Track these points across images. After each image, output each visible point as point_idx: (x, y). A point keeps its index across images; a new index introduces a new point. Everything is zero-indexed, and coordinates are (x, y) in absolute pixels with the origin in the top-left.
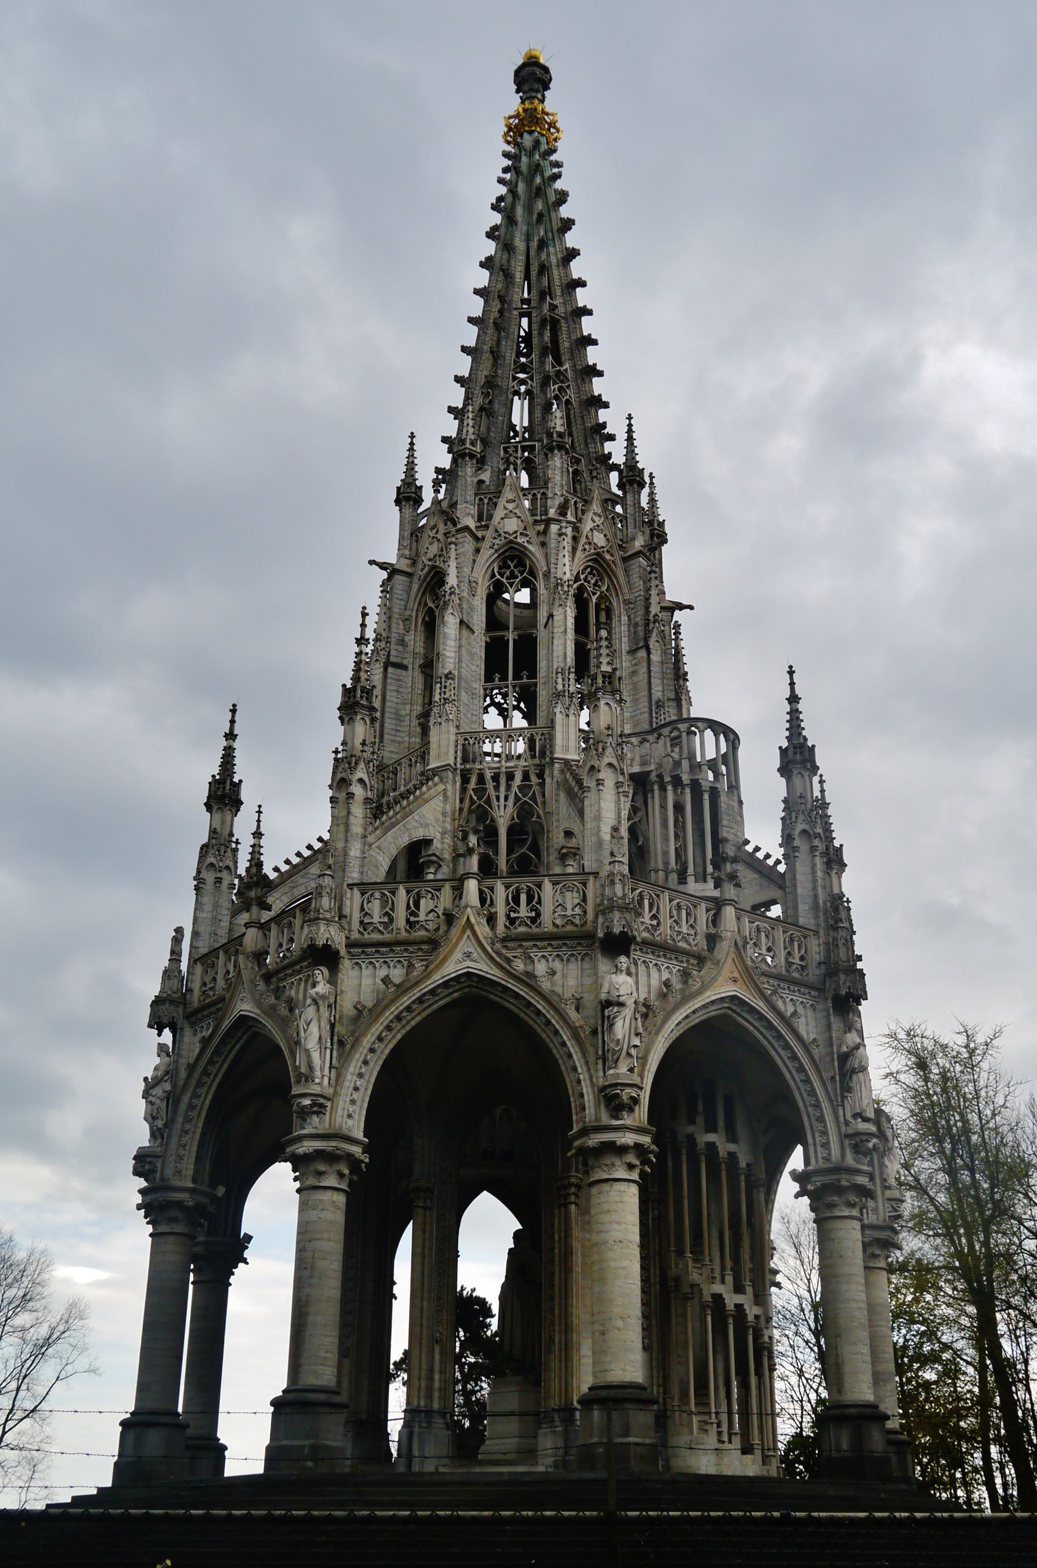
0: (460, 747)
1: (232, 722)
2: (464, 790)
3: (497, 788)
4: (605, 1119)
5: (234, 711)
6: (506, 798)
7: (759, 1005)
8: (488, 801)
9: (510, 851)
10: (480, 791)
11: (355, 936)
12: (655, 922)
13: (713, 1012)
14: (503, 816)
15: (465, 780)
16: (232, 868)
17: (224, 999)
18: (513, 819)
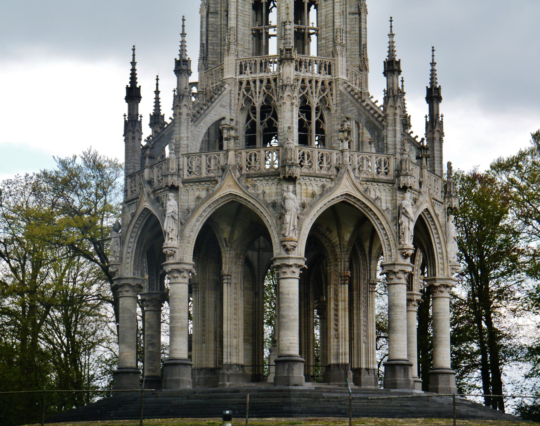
0: (238, 67)
1: (134, 55)
2: (240, 90)
3: (255, 87)
4: (284, 254)
5: (134, 50)
6: (260, 92)
7: (359, 196)
8: (252, 95)
9: (262, 117)
10: (248, 90)
11: (186, 177)
12: (310, 164)
14: (258, 101)
15: (241, 83)
16: (139, 130)
17: (138, 198)
18: (263, 103)
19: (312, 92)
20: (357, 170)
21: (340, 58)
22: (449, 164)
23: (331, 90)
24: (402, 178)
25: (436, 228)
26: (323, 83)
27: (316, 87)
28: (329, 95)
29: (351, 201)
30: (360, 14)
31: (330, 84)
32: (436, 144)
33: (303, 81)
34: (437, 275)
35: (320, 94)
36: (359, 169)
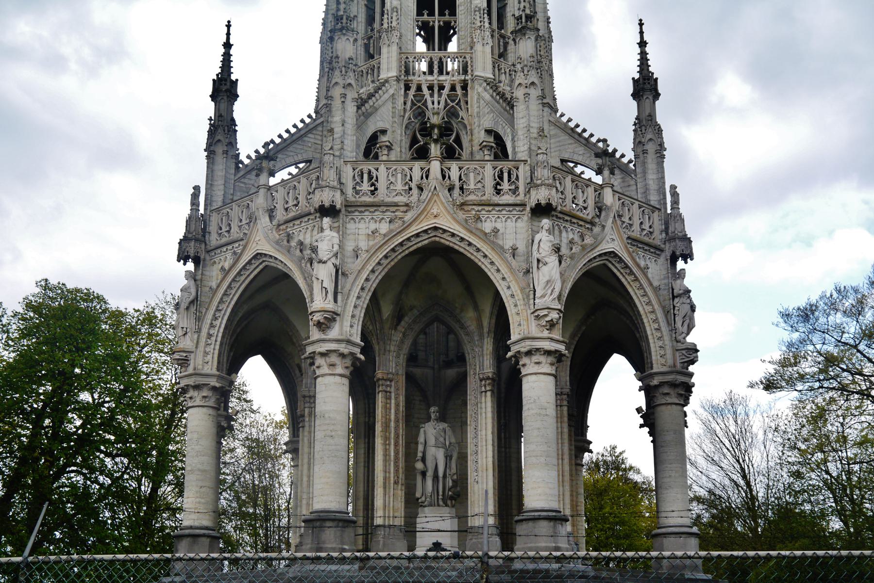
12: (373, 188)
13: (424, 241)
19: (433, 103)
20: (457, 191)
21: (478, 47)
22: (673, 188)
23: (466, 95)
24: (533, 192)
25: (641, 287)
26: (453, 88)
27: (440, 95)
28: (462, 103)
29: (447, 240)
31: (465, 87)
32: (651, 158)
33: (419, 88)
34: (654, 366)
35: (446, 104)
36: (461, 188)
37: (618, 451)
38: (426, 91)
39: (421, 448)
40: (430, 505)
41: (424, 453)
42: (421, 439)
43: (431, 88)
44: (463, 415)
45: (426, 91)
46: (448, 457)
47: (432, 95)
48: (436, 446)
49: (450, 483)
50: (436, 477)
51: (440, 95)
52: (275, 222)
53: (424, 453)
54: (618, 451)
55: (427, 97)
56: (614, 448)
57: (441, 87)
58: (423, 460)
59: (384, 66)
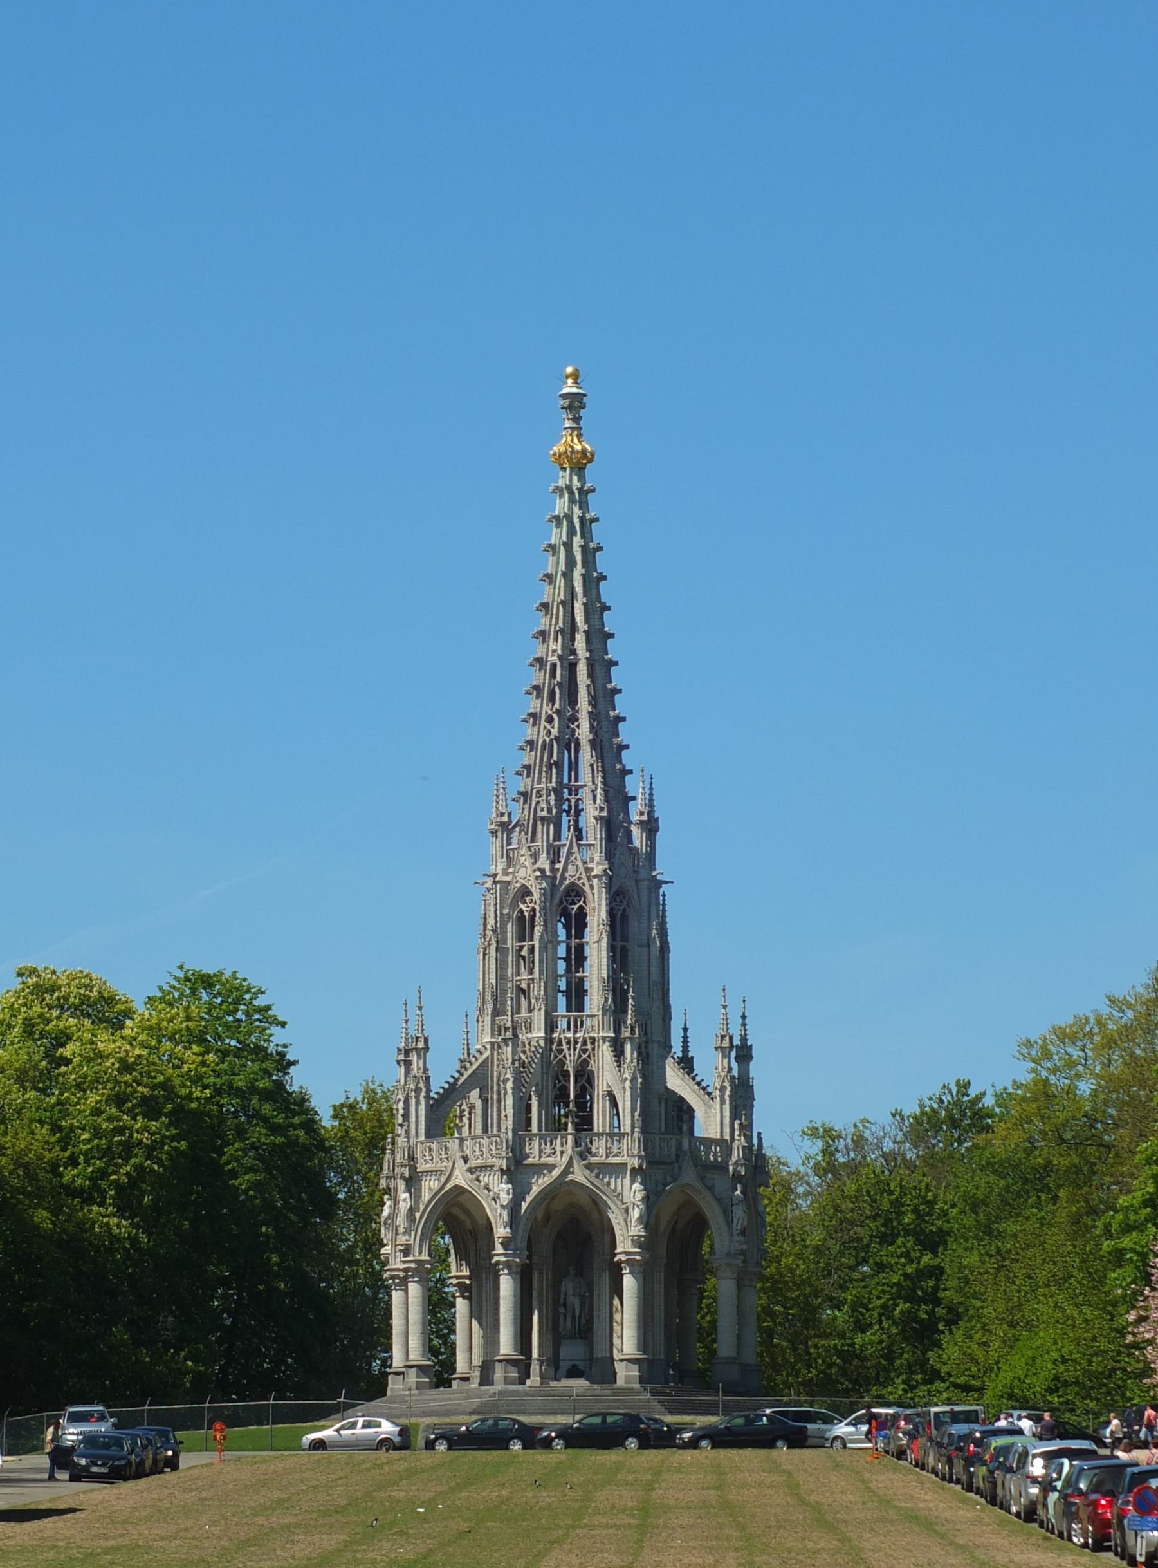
23: (593, 1049)
26: (584, 1043)
27: (575, 1049)
30: (649, 947)
31: (593, 1043)
35: (580, 1056)
37: (973, 1092)
38: (565, 1047)
39: (562, 1296)
40: (571, 1338)
41: (565, 1299)
42: (563, 1289)
43: (569, 1043)
44: (623, 1015)
45: (565, 1047)
46: (582, 1305)
47: (569, 1049)
48: (574, 1295)
49: (583, 1321)
50: (574, 1317)
51: (575, 1049)
52: (468, 1165)
53: (565, 1299)
54: (973, 1092)
55: (566, 1050)
56: (968, 1084)
57: (576, 1042)
58: (565, 1305)
59: (535, 1025)
